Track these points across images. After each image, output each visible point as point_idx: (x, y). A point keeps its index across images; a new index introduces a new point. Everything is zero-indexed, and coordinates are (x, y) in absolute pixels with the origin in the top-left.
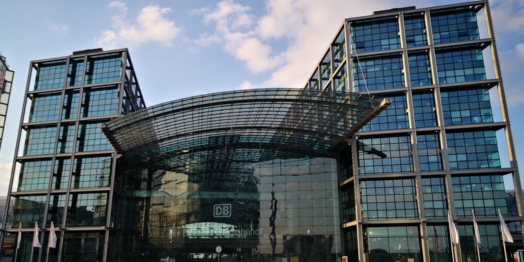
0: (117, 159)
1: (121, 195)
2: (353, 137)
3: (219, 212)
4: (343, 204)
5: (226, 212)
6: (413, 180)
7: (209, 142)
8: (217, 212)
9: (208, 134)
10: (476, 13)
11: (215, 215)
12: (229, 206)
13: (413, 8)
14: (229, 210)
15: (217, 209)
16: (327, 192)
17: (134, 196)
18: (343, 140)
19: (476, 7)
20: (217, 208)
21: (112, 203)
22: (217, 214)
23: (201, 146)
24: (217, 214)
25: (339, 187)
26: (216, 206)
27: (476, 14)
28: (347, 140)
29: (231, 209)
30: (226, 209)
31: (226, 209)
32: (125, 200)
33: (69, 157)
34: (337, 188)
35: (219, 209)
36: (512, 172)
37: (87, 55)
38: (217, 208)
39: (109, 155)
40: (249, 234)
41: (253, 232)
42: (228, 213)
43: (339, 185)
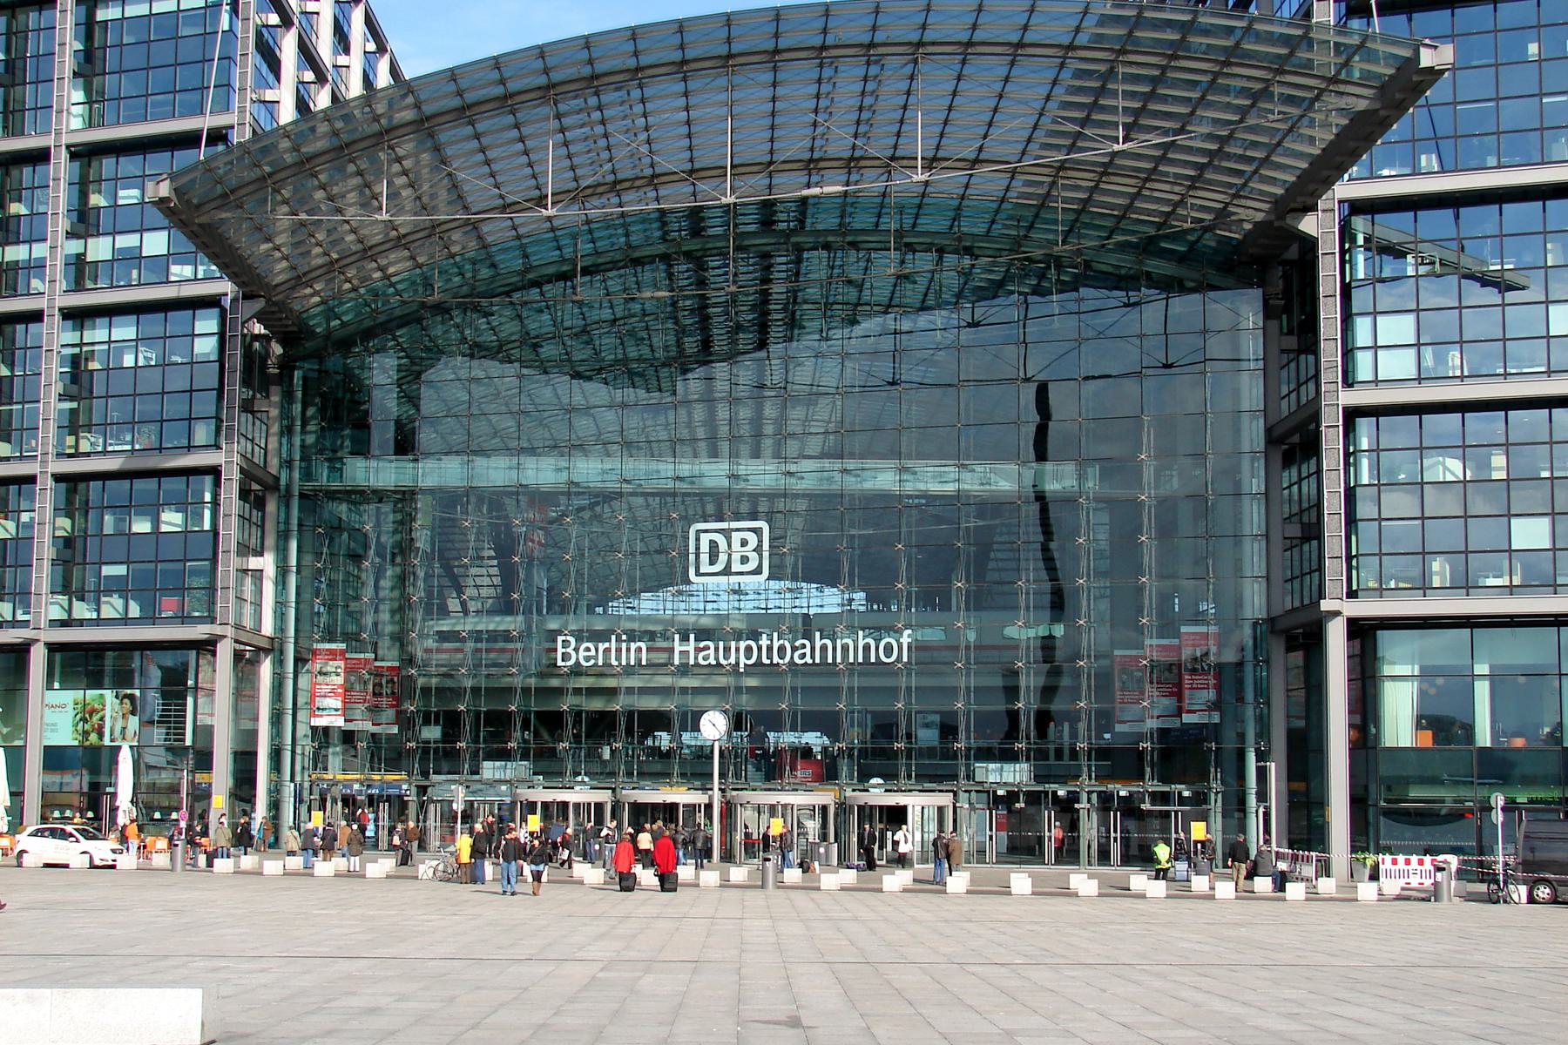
1: (277, 479)
3: (712, 563)
5: (744, 560)
8: (705, 558)
11: (698, 574)
12: (757, 531)
14: (758, 550)
15: (705, 547)
20: (705, 538)
30: (744, 543)
31: (744, 543)
33: (36, 316)
34: (1260, 444)
35: (714, 545)
42: (752, 565)
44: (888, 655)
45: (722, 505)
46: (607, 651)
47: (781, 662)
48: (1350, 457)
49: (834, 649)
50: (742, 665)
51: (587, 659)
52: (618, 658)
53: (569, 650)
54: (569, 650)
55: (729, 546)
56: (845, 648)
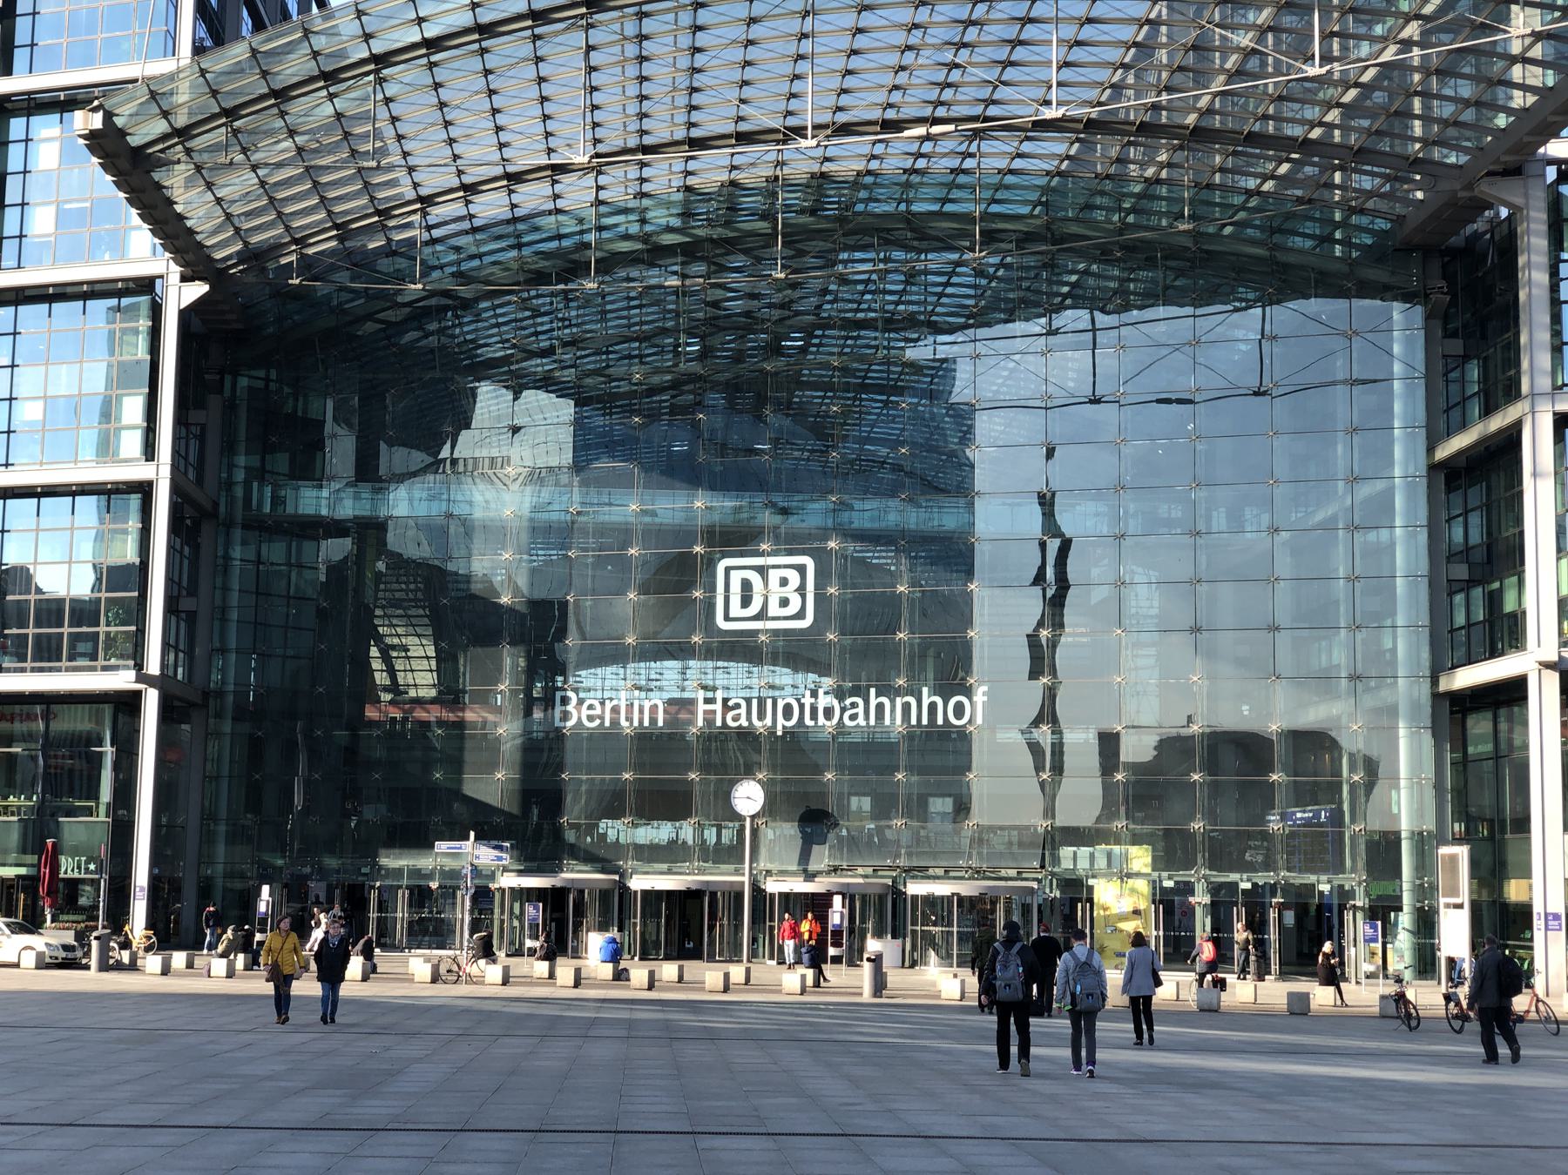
0: (185, 315)
1: (216, 504)
2: (1531, 168)
3: (746, 601)
4: (1452, 557)
5: (784, 602)
7: (687, 215)
11: (727, 618)
12: (801, 569)
14: (801, 590)
15: (736, 587)
16: (1365, 490)
17: (290, 510)
18: (1469, 186)
20: (736, 577)
21: (171, 548)
22: (736, 610)
23: (645, 238)
24: (736, 610)
25: (1433, 468)
26: (728, 570)
28: (1486, 189)
30: (784, 582)
31: (784, 582)
32: (237, 533)
34: (1422, 470)
35: (746, 586)
38: (736, 577)
39: (145, 285)
40: (914, 721)
41: (933, 707)
43: (1431, 450)
46: (615, 710)
47: (828, 723)
49: (893, 710)
50: (779, 727)
51: (591, 718)
52: (629, 719)
53: (570, 708)
54: (570, 708)
55: (766, 584)
56: (906, 707)
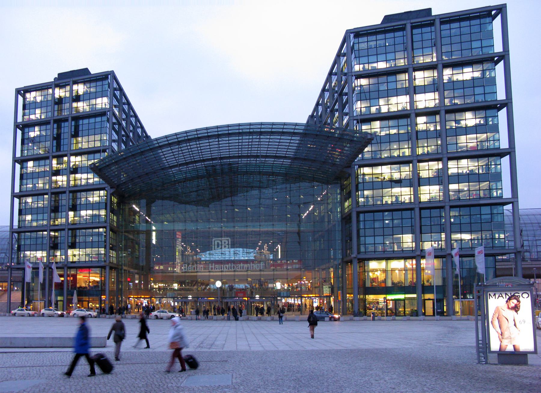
2: (352, 166)
3: (218, 246)
6: (413, 211)
9: (203, 163)
10: (493, 19)
12: (228, 240)
13: (428, 11)
15: (216, 244)
19: (493, 12)
27: (493, 22)
28: (345, 170)
29: (230, 243)
30: (225, 243)
31: (225, 243)
35: (218, 243)
36: (512, 203)
37: (71, 80)
44: (258, 267)
45: (220, 235)
48: (358, 221)
